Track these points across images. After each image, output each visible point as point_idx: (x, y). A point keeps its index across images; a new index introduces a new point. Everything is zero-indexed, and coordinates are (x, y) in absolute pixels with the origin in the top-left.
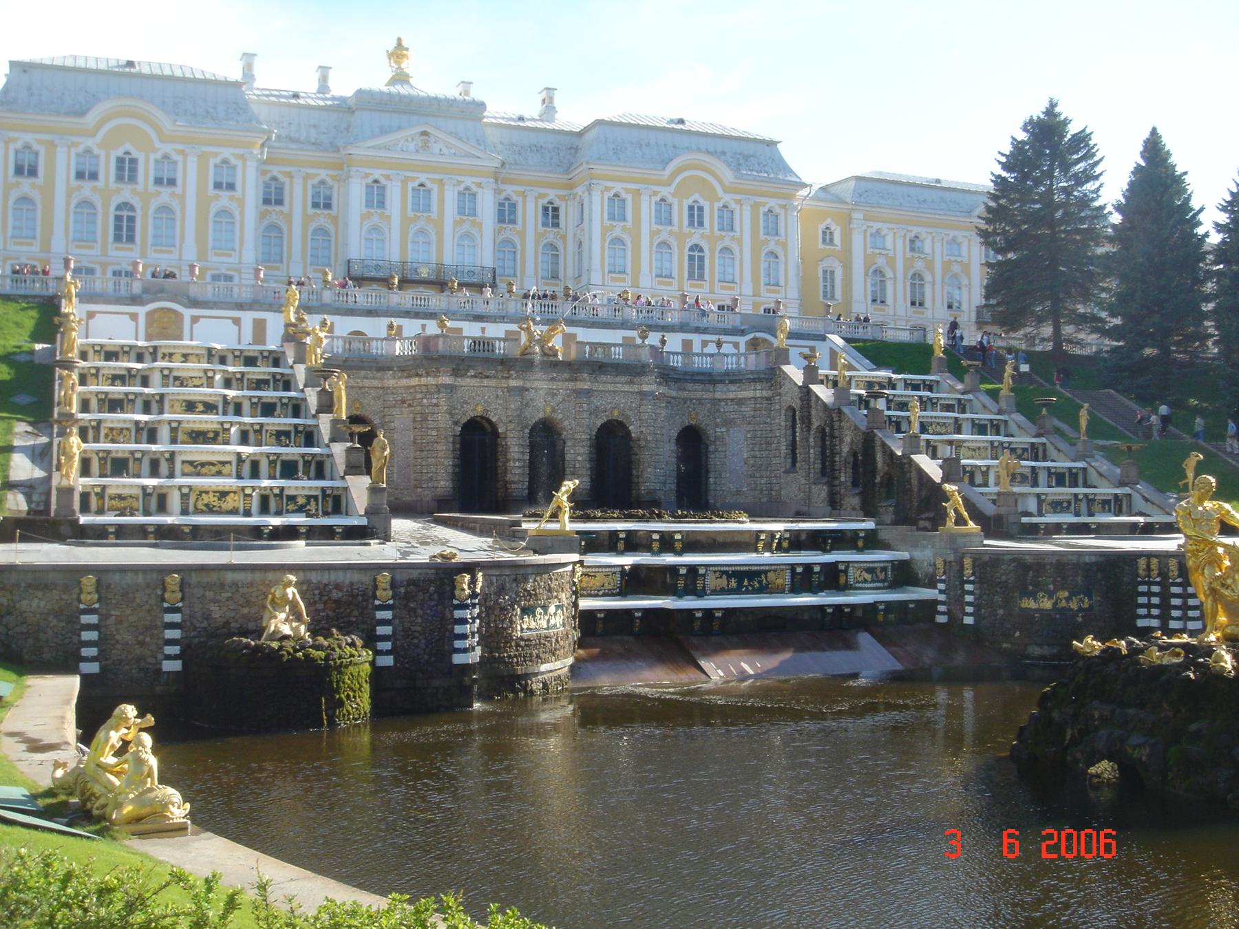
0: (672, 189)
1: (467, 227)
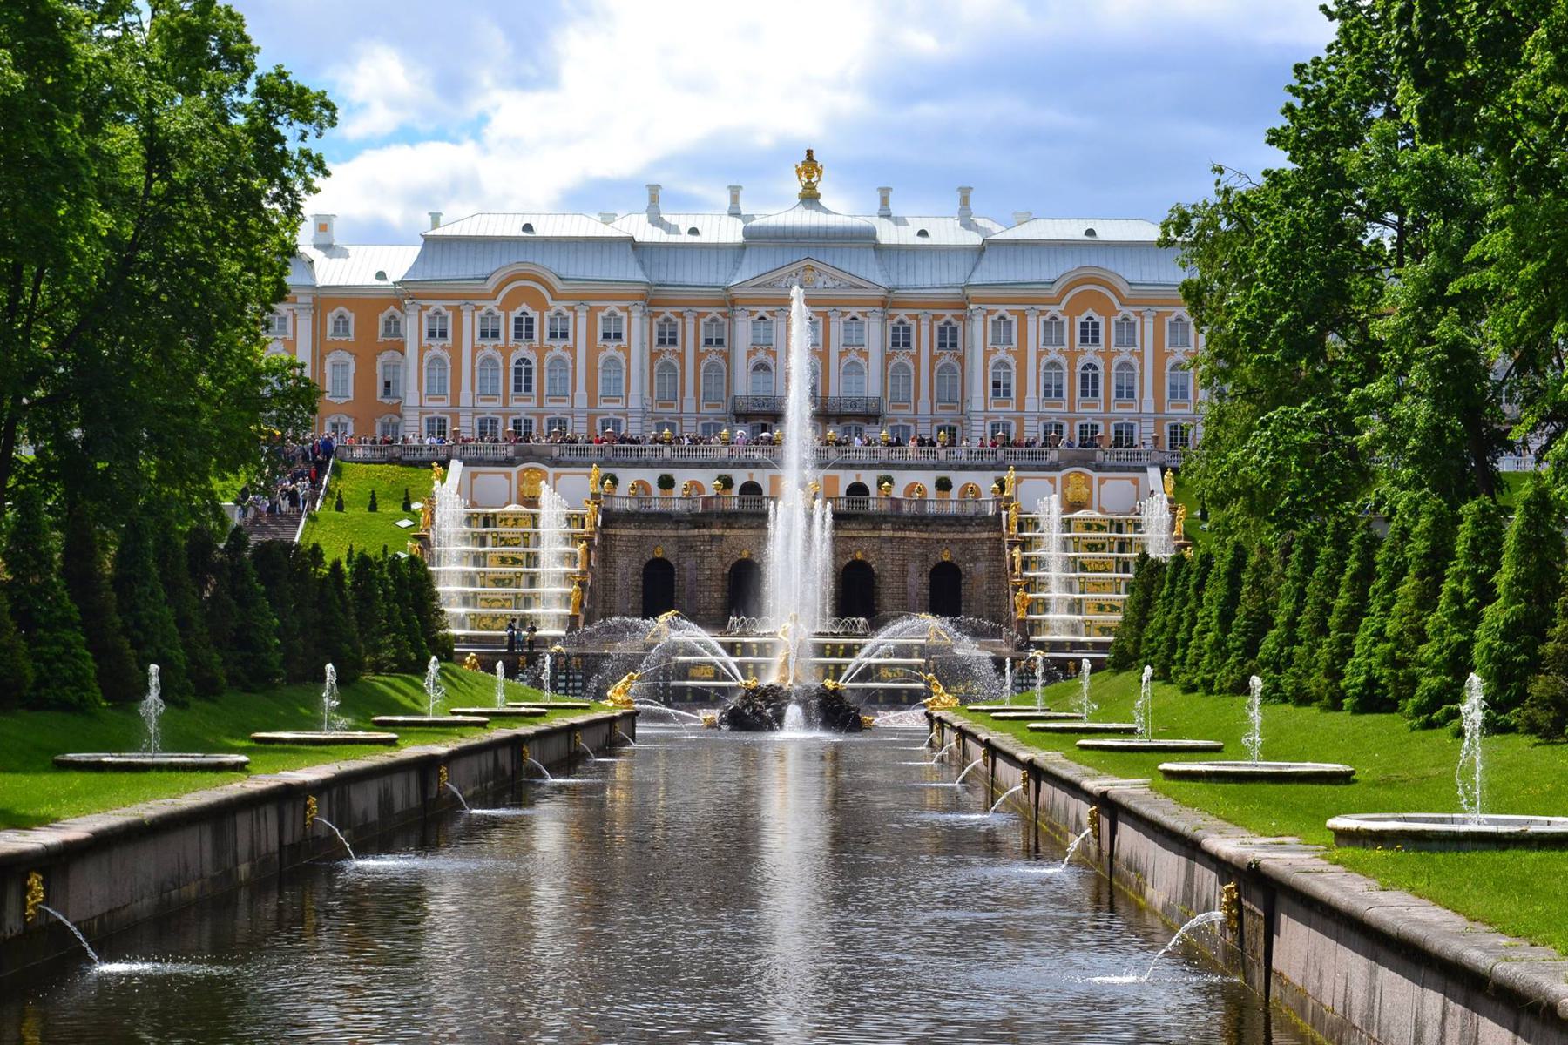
0: (1063, 306)
1: (853, 356)
